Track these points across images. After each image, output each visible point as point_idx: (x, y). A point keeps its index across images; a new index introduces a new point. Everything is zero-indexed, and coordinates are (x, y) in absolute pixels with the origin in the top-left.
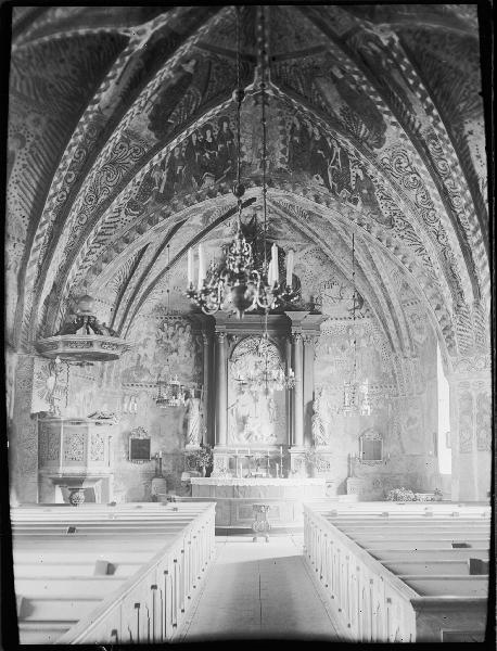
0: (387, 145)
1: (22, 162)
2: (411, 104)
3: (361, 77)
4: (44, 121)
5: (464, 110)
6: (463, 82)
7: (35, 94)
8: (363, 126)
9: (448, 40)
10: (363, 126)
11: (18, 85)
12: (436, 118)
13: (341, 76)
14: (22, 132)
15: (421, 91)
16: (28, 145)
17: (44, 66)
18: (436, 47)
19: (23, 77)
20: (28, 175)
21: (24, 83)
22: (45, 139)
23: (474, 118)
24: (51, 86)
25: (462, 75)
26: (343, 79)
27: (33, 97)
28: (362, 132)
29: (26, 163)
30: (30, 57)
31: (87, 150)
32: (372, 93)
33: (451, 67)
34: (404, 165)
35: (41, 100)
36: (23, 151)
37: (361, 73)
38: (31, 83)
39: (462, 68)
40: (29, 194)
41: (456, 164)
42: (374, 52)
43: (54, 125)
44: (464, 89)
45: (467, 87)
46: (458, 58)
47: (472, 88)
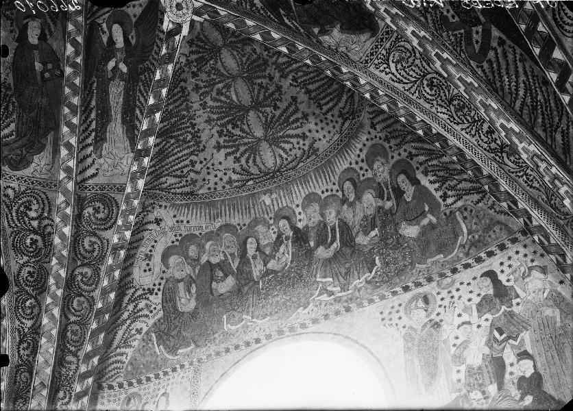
0: (27, 172)
2: (104, 139)
3: (77, 53)
5: (167, 190)
6: (192, 153)
8: (13, 126)
9: (214, 94)
10: (13, 126)
12: (142, 172)
13: (33, 38)
15: (152, 121)
18: (197, 88)
23: (173, 205)
25: (198, 143)
26: (35, 47)
28: (6, 131)
32: (72, 86)
33: (193, 126)
34: (33, 214)
37: (82, 49)
39: (204, 137)
41: (122, 248)
42: (111, 41)
44: (187, 162)
45: (193, 163)
46: (209, 121)
47: (198, 167)
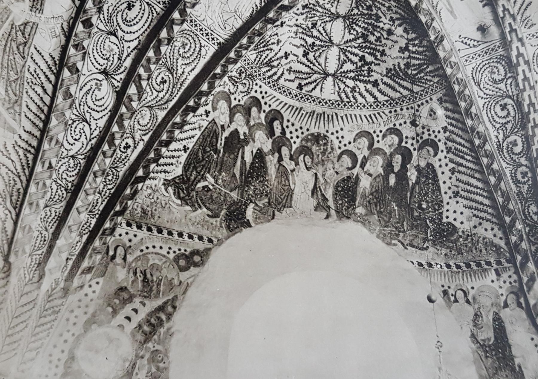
1: (446, 169)
4: (436, 105)
7: (405, 88)
11: (378, 94)
14: (425, 137)
16: (441, 146)
17: (383, 53)
19: (375, 84)
20: (464, 178)
21: (382, 86)
22: (451, 124)
24: (408, 65)
27: (405, 92)
29: (451, 165)
30: (362, 58)
31: (510, 97)
35: (416, 89)
36: (441, 155)
38: (386, 79)
40: (480, 199)
43: (446, 101)
